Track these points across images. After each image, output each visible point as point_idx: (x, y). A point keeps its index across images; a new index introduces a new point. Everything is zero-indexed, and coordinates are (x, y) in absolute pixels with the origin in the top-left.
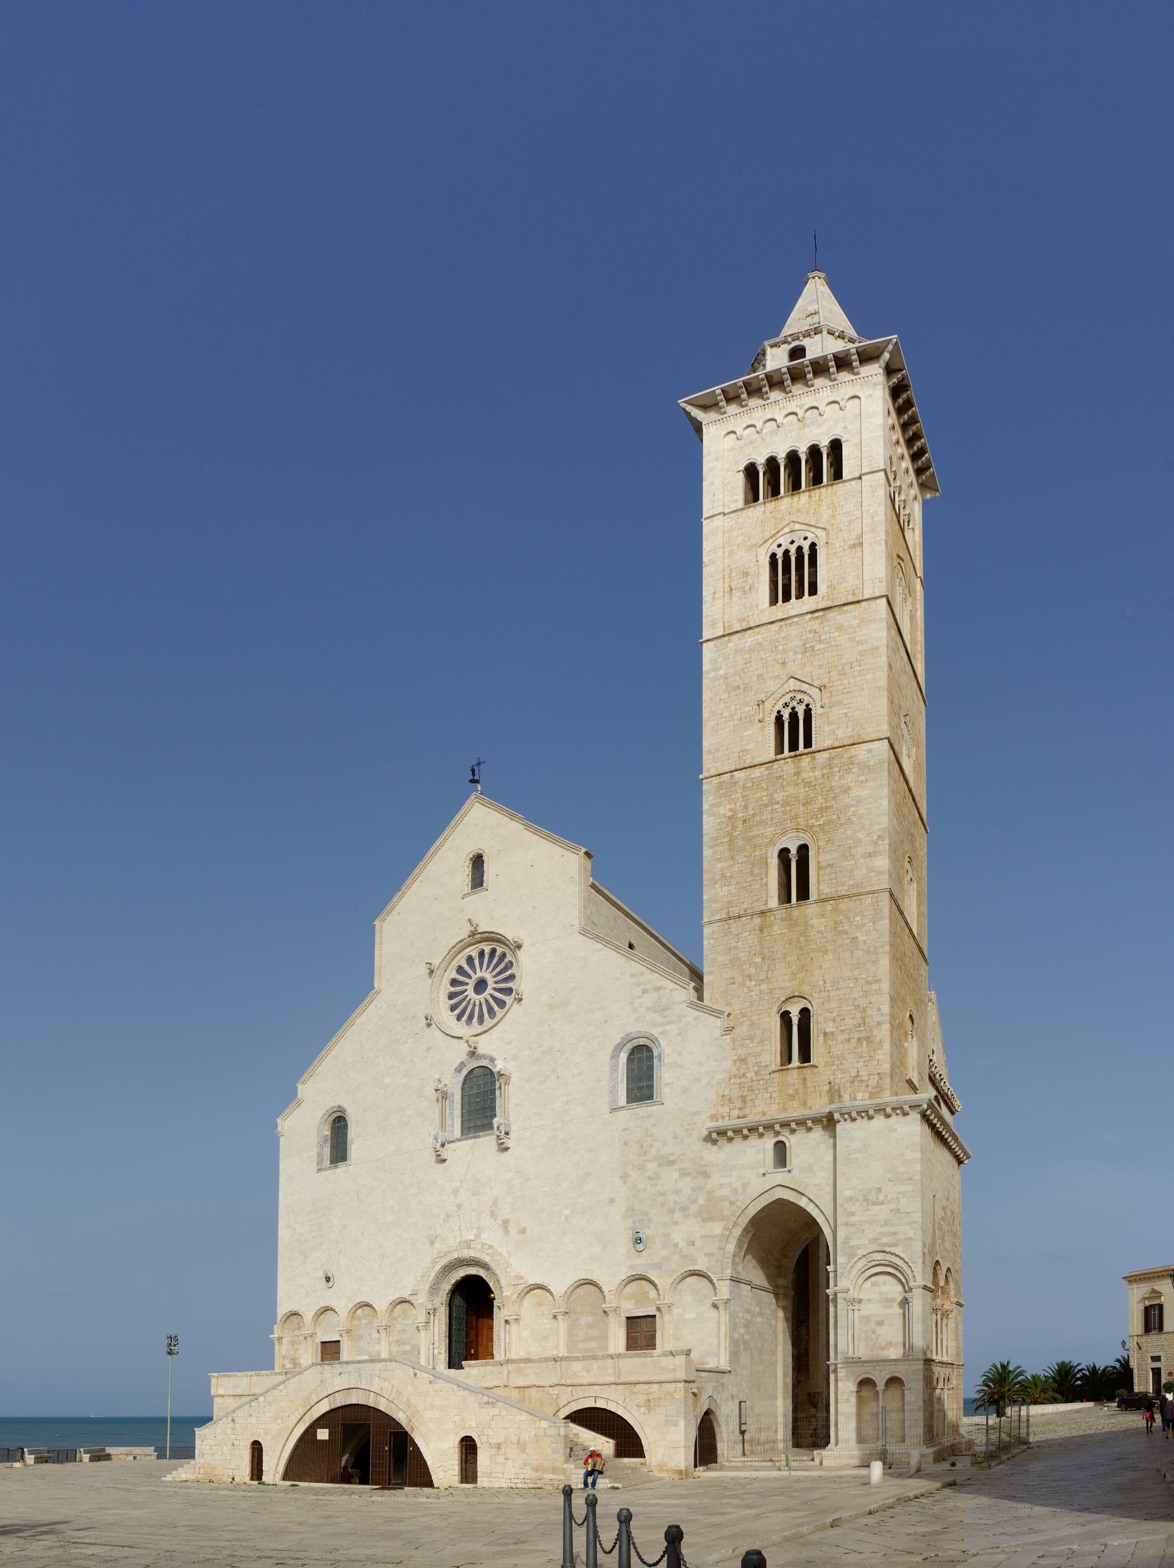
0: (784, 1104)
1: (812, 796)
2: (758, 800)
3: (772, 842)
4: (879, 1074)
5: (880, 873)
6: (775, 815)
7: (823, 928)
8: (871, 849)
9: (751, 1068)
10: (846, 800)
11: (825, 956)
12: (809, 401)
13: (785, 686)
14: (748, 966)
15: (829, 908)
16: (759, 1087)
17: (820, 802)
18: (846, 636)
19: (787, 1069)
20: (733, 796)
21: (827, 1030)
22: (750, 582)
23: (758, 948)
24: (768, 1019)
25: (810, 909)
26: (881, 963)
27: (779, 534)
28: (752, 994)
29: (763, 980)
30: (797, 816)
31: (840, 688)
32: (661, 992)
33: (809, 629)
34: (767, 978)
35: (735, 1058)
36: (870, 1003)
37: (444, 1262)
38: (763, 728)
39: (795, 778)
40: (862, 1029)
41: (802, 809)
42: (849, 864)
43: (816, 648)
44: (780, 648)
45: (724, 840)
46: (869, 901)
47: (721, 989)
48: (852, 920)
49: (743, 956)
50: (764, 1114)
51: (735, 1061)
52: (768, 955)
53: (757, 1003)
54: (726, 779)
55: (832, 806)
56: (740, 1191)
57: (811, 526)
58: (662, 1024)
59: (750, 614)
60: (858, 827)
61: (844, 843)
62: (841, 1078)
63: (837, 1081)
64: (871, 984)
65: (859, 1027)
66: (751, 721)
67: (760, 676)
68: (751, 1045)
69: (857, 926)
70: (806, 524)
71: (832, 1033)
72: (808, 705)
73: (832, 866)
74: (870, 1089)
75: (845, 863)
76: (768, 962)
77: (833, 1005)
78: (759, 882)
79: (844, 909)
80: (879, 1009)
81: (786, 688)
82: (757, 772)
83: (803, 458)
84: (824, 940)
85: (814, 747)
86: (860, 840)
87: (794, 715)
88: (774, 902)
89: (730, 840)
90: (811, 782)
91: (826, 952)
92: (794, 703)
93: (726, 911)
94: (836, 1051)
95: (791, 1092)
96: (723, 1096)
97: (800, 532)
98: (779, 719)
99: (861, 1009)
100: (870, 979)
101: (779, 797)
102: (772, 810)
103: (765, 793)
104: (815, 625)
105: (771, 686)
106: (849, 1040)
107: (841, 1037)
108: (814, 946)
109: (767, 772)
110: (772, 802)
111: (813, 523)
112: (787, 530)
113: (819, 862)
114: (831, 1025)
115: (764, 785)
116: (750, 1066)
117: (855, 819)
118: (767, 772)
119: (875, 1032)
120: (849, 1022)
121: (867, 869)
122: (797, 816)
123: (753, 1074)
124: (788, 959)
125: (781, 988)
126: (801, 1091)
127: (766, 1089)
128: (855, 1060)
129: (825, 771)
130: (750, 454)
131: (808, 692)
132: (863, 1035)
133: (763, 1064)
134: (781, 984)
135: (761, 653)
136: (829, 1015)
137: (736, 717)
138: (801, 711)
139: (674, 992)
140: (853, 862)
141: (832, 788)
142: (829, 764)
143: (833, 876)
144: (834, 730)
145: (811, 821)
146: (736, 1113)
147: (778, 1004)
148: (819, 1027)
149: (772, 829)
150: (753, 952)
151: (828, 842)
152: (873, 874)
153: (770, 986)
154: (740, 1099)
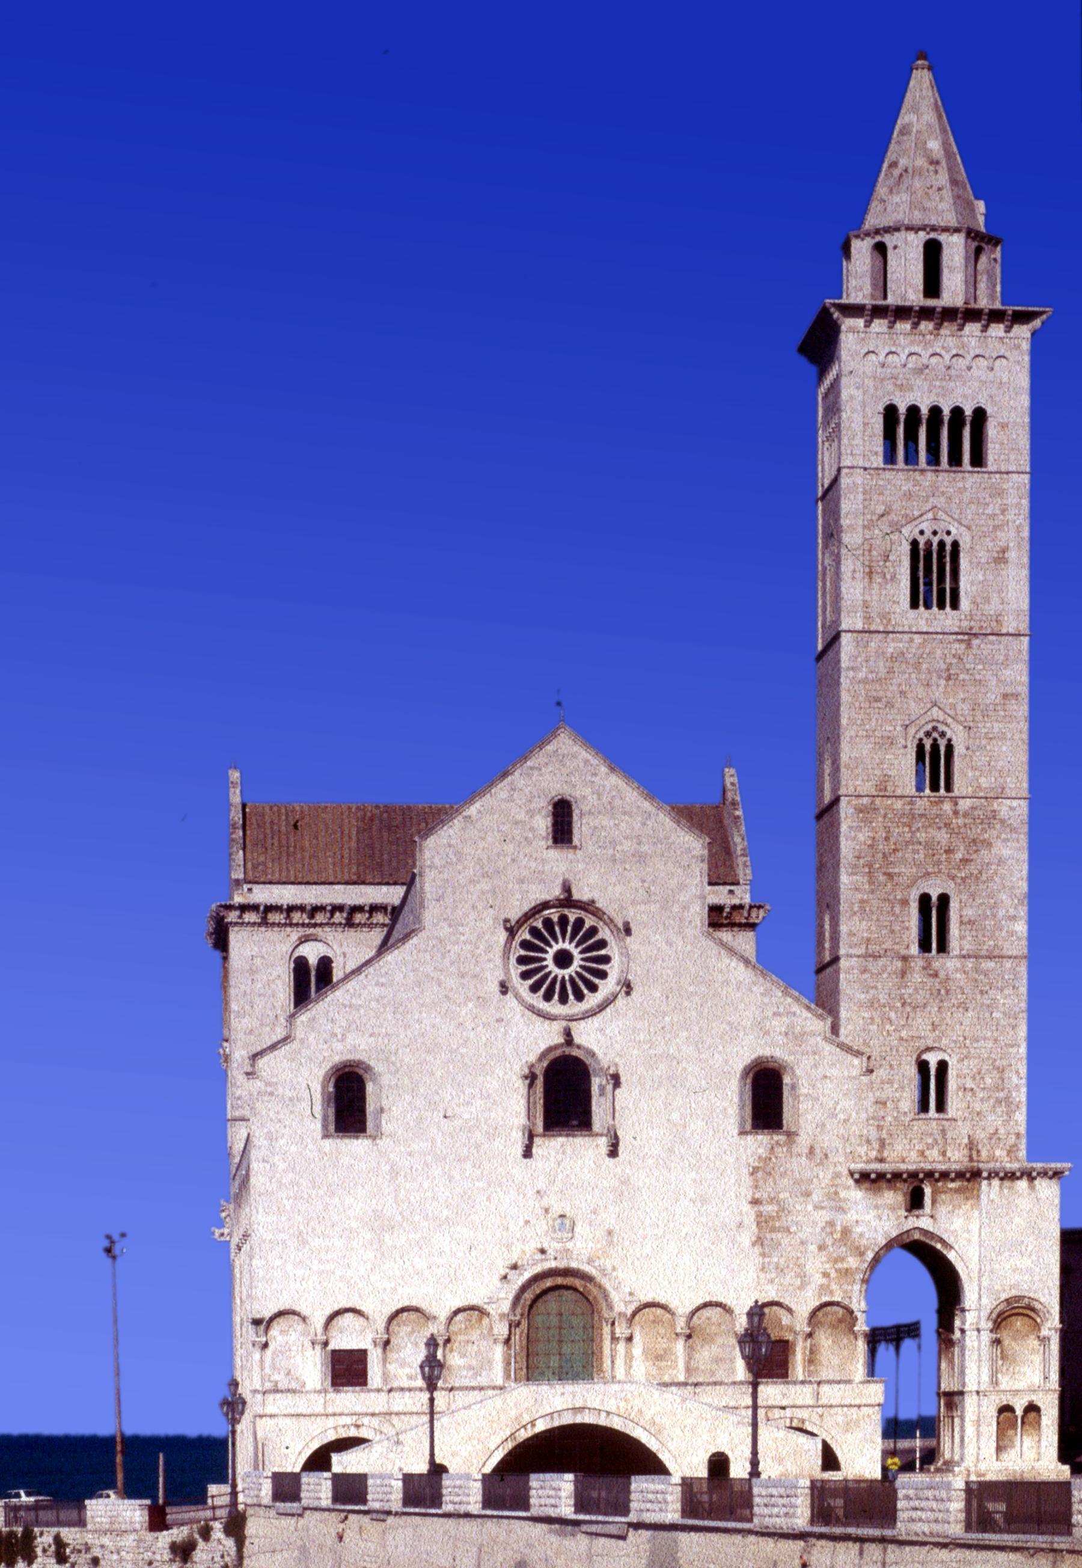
5: (1019, 939)
21: (968, 1086)
62: (981, 1135)
71: (972, 1090)
85: (956, 792)
87: (935, 746)
92: (935, 735)
98: (920, 747)
132: (1001, 1095)
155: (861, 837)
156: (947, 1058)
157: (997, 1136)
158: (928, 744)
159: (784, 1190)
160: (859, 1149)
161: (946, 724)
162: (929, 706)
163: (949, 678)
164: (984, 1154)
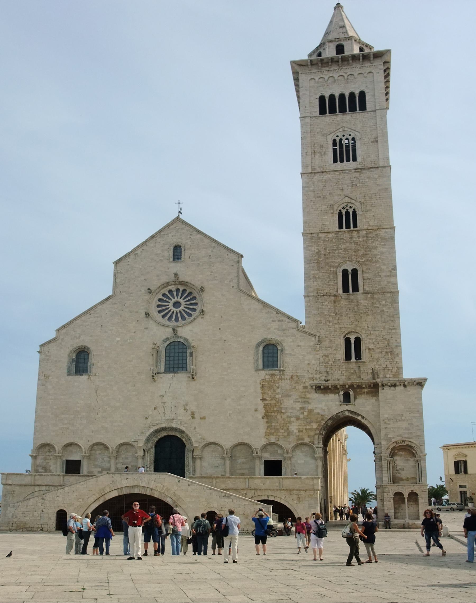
0: (349, 376)
1: (358, 248)
2: (331, 247)
3: (339, 265)
4: (397, 367)
6: (340, 254)
7: (366, 305)
8: (389, 274)
9: (331, 360)
10: (375, 252)
11: (368, 316)
12: (349, 71)
13: (344, 200)
14: (328, 316)
15: (369, 296)
16: (336, 368)
17: (362, 251)
18: (372, 182)
19: (350, 362)
20: (319, 244)
22: (324, 151)
23: (333, 310)
24: (340, 340)
25: (359, 296)
26: (396, 321)
27: (337, 131)
28: (331, 328)
29: (336, 323)
30: (351, 256)
31: (370, 204)
32: (282, 322)
33: (354, 176)
34: (338, 323)
35: (323, 355)
36: (392, 338)
37: (156, 428)
38: (333, 216)
39: (350, 240)
40: (388, 348)
41: (354, 253)
42: (378, 279)
43: (358, 185)
44: (340, 182)
45: (314, 262)
46: (389, 295)
47: (314, 325)
48: (380, 302)
49: (326, 312)
50: (338, 380)
51: (322, 356)
52: (338, 313)
53: (333, 333)
54: (314, 236)
55: (369, 254)
56: (326, 411)
57: (352, 130)
58: (283, 336)
59: (324, 165)
60: (382, 264)
61: (375, 270)
63: (376, 369)
64: (391, 330)
65: (386, 347)
66: (327, 212)
67: (331, 194)
68: (330, 350)
69: (383, 305)
70: (350, 129)
71: (373, 349)
72: (354, 209)
73: (370, 279)
74: (393, 373)
75: (376, 279)
76: (338, 316)
77: (372, 337)
78: (333, 282)
79: (377, 297)
80: (396, 340)
81: (344, 201)
82: (330, 235)
83: (347, 97)
84: (367, 310)
85: (358, 228)
86: (383, 269)
87: (347, 213)
88: (340, 291)
89: (318, 262)
90: (358, 243)
91: (368, 315)
92: (348, 208)
93: (316, 292)
94: (376, 356)
95: (352, 371)
96: (316, 370)
97: (347, 132)
98: (340, 214)
99: (387, 340)
100: (391, 327)
101: (342, 247)
102: (339, 252)
103: (335, 244)
104: (357, 175)
105: (336, 198)
106: (381, 352)
107: (377, 351)
108: (362, 312)
109: (336, 236)
110: (338, 249)
111: (353, 128)
112: (341, 130)
113: (363, 277)
114: (372, 345)
115: (334, 241)
116: (330, 359)
117: (380, 261)
118: (336, 236)
119: (395, 350)
120: (381, 345)
121: (387, 282)
122: (351, 256)
123: (332, 363)
124: (349, 316)
125: (345, 328)
126: (357, 371)
127: (339, 369)
128: (386, 361)
129: (364, 239)
130: (322, 91)
131: (355, 203)
132: (389, 350)
133: (337, 359)
134: (346, 326)
135: (331, 183)
136: (370, 341)
137: (319, 209)
138: (351, 211)
139: (289, 324)
140: (380, 278)
141: (368, 246)
142: (367, 236)
143: (370, 283)
144: (368, 222)
145: (359, 259)
146: (323, 378)
147: (344, 334)
148: (366, 345)
149: (339, 260)
150: (331, 311)
151: (367, 269)
152: (390, 284)
153: (340, 326)
154: (326, 373)
155: (313, 249)
156: (359, 336)
157: (387, 369)
158: (344, 212)
159: (277, 394)
160: (316, 376)
161: (352, 203)
162: (343, 197)
163: (353, 186)
164: (381, 376)
